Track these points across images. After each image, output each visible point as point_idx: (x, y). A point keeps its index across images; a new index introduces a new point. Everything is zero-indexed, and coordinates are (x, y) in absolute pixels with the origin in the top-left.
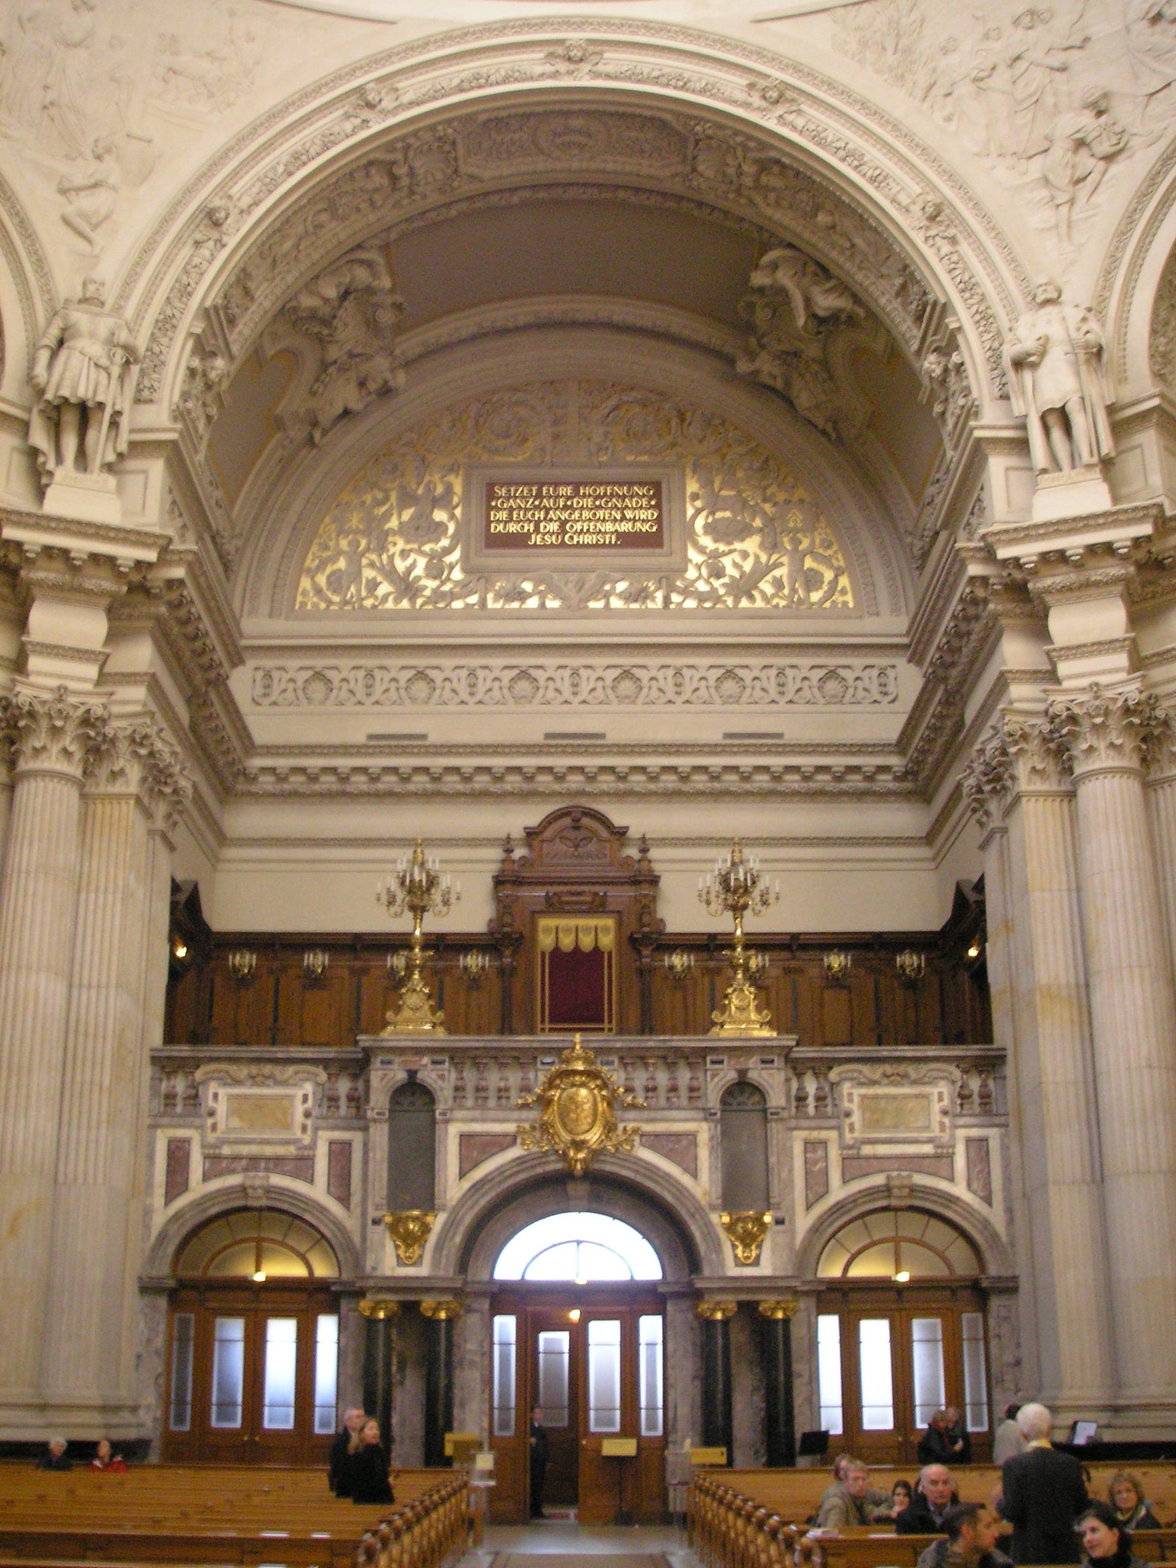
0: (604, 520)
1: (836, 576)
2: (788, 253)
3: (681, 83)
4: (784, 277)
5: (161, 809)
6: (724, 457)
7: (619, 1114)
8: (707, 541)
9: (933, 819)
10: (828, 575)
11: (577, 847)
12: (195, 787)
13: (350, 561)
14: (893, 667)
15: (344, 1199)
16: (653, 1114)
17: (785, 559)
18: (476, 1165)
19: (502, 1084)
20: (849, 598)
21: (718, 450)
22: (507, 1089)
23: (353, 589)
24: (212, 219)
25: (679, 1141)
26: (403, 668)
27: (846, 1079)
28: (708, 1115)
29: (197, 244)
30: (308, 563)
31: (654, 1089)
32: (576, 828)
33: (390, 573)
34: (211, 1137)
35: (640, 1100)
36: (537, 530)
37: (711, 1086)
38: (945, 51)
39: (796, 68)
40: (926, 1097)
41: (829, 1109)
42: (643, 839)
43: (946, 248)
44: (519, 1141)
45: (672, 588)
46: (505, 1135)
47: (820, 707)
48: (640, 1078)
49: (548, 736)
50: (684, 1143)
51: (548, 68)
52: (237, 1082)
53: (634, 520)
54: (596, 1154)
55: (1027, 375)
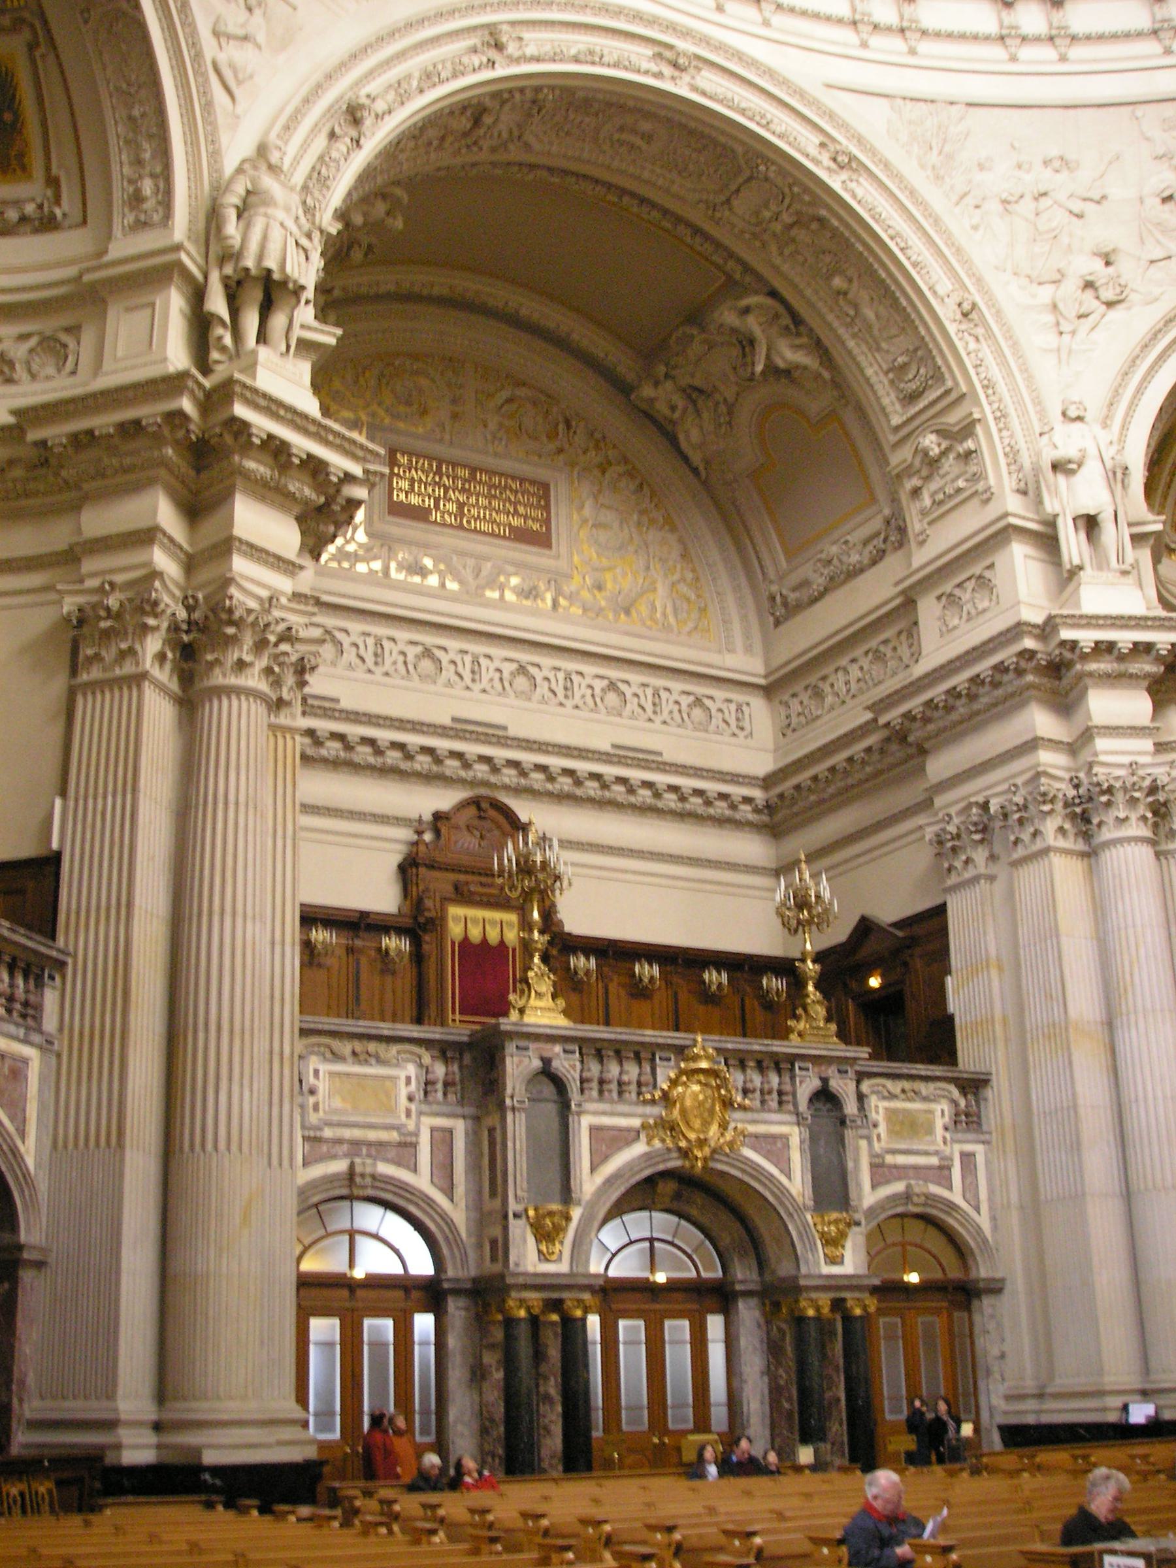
2: (769, 301)
3: (764, 122)
4: (753, 324)
6: (604, 472)
15: (449, 1192)
16: (756, 1116)
18: (606, 1158)
24: (354, 115)
28: (800, 1120)
29: (332, 135)
34: (313, 1118)
37: (799, 1092)
38: (981, 167)
39: (860, 140)
43: (972, 345)
44: (643, 1136)
46: (629, 1130)
49: (454, 719)
50: (779, 1145)
51: (654, 67)
55: (1061, 479)
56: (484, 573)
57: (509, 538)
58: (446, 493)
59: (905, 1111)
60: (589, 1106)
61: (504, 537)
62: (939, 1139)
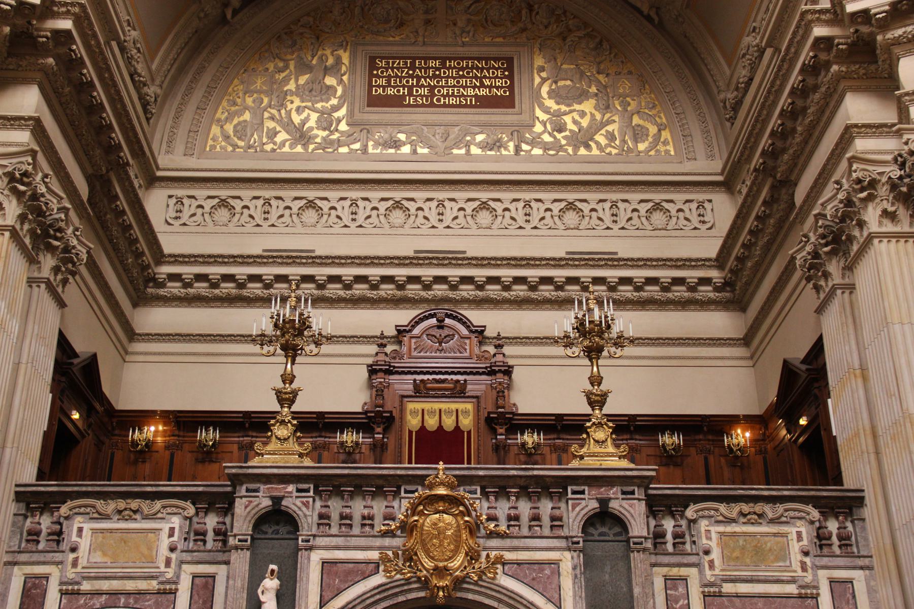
0: (467, 87)
1: (659, 130)
5: (48, 262)
6: (564, 39)
7: (481, 541)
8: (550, 103)
9: (750, 322)
10: (653, 130)
11: (440, 343)
12: (88, 252)
13: (254, 115)
14: (710, 201)
16: (516, 543)
17: (616, 118)
19: (366, 512)
20: (670, 148)
21: (561, 33)
22: (371, 518)
23: (255, 136)
25: (543, 570)
26: (296, 198)
27: (703, 517)
28: (571, 545)
30: (218, 115)
31: (517, 518)
32: (440, 327)
33: (288, 125)
34: (71, 574)
35: (503, 528)
36: (410, 94)
37: (572, 515)
40: (784, 535)
41: (688, 547)
42: (498, 337)
44: (382, 568)
45: (522, 140)
46: (367, 562)
47: (648, 233)
48: (503, 508)
49: (416, 252)
50: (547, 572)
52: (105, 517)
53: (490, 87)
54: (459, 583)
56: (452, 137)
57: (475, 106)
58: (418, 82)
59: (753, 535)
60: (320, 541)
61: (471, 106)
62: (796, 566)
